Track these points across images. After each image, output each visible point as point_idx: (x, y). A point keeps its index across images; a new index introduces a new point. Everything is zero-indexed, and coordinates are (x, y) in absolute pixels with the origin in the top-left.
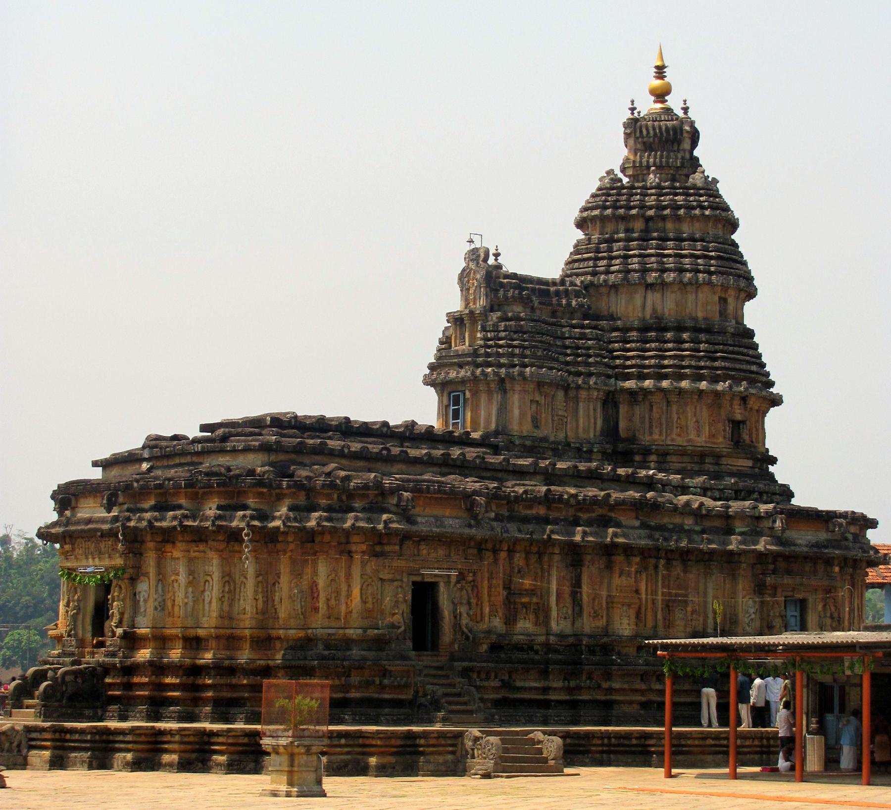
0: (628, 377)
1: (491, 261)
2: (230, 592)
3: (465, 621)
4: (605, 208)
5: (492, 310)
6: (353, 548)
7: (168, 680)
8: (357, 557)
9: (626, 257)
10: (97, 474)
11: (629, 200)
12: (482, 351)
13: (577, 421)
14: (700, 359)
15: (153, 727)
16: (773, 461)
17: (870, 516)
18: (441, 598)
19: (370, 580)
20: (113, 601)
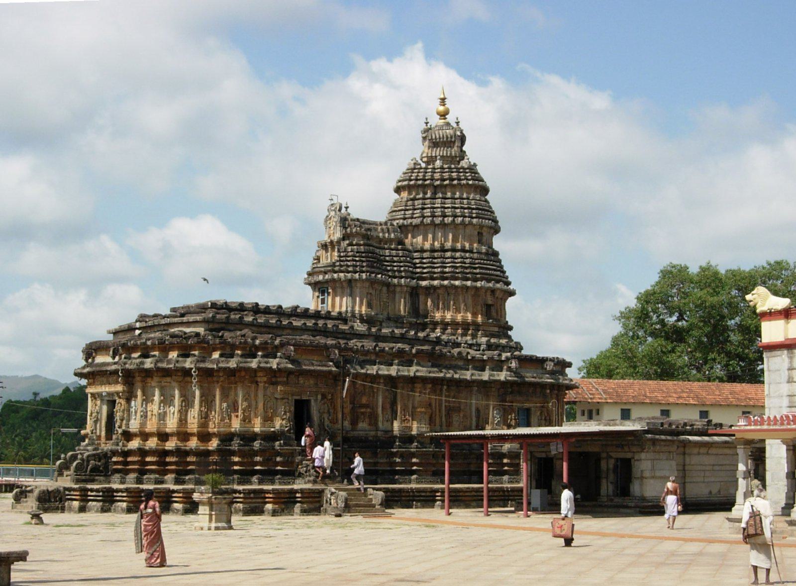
0: (424, 279)
1: (343, 210)
2: (185, 406)
3: (327, 422)
4: (411, 180)
5: (344, 239)
6: (259, 379)
7: (148, 459)
8: (261, 385)
9: (423, 209)
10: (110, 337)
11: (424, 176)
12: (338, 264)
14: (466, 268)
15: (138, 488)
16: (511, 328)
17: (568, 360)
18: (312, 408)
19: (269, 399)
20: (117, 412)
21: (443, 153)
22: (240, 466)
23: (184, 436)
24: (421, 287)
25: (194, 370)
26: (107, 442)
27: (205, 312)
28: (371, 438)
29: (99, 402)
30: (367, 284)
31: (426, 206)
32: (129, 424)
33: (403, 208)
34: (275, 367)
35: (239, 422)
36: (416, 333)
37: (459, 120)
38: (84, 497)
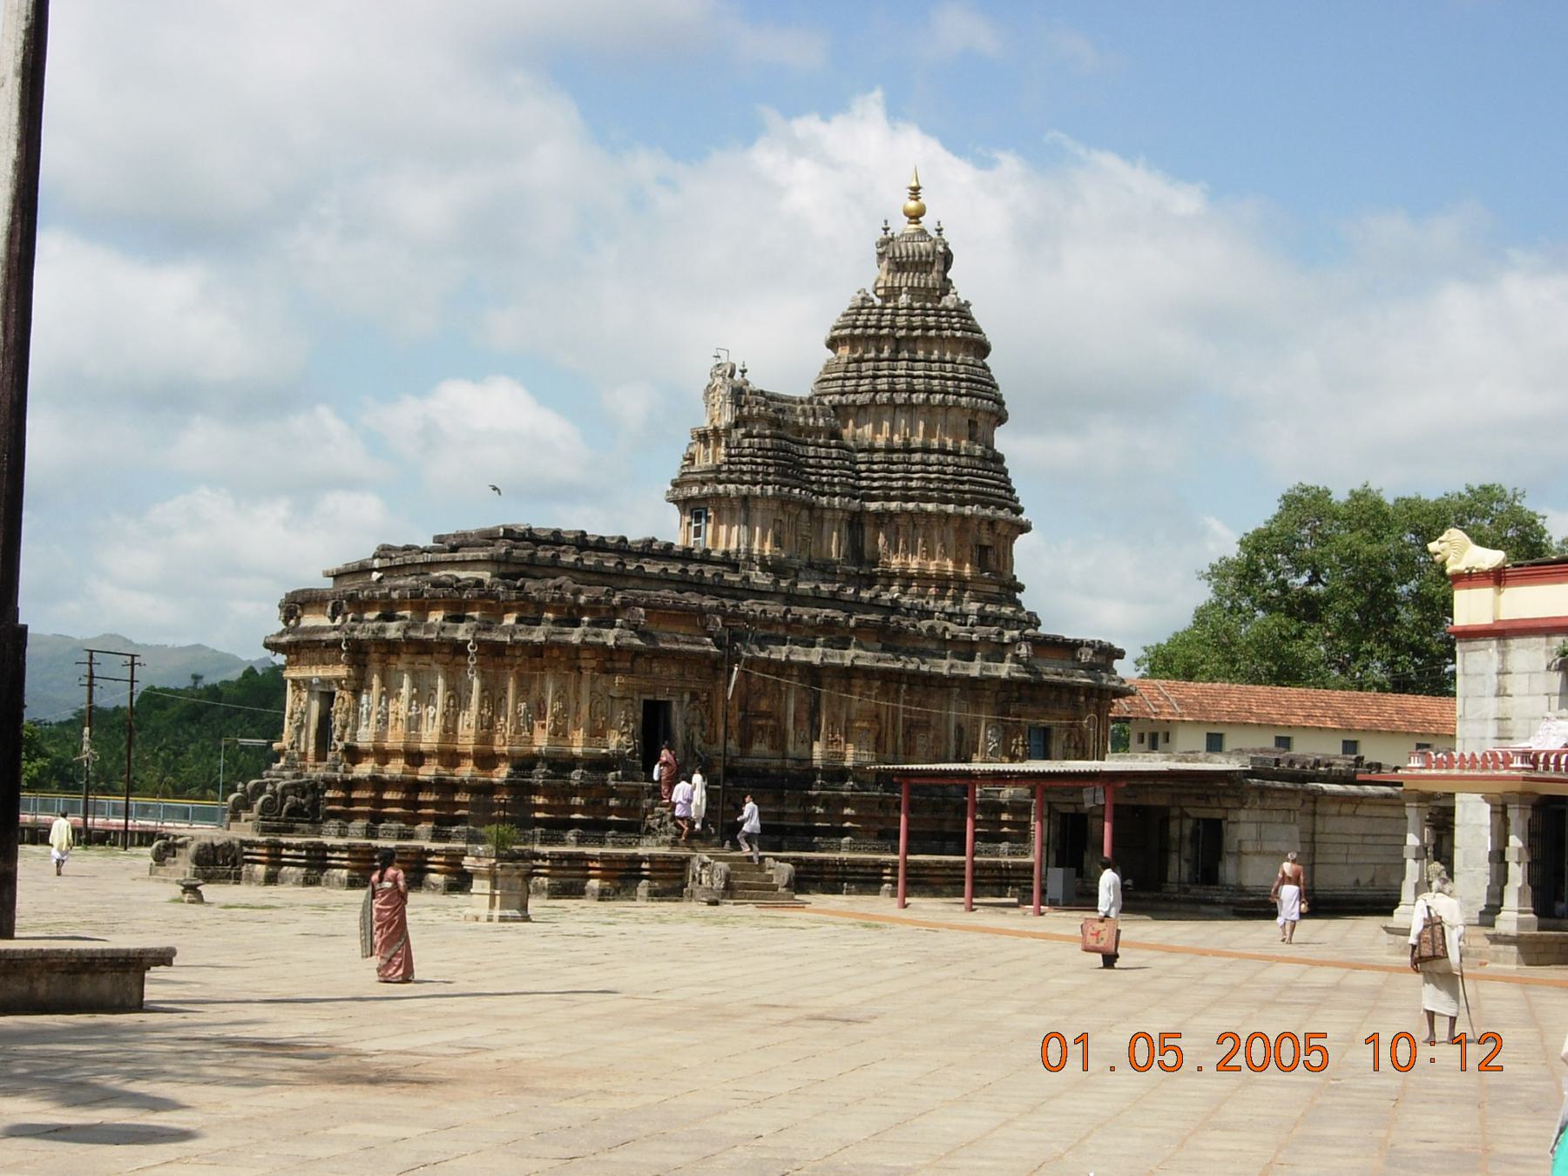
0: (874, 499)
1: (738, 375)
2: (454, 706)
3: (698, 741)
4: (856, 327)
5: (737, 425)
6: (583, 664)
7: (388, 796)
8: (587, 673)
9: (875, 377)
11: (879, 321)
12: (725, 468)
13: (821, 543)
14: (947, 482)
16: (1021, 588)
17: (1118, 646)
18: (673, 716)
21: (913, 282)
22: (546, 813)
23: (451, 757)
24: (868, 512)
25: (471, 644)
26: (318, 764)
27: (493, 545)
28: (773, 771)
29: (305, 695)
30: (775, 505)
31: (880, 373)
32: (355, 735)
33: (841, 374)
34: (611, 642)
35: (547, 736)
36: (857, 592)
37: (942, 226)
38: (275, 858)
